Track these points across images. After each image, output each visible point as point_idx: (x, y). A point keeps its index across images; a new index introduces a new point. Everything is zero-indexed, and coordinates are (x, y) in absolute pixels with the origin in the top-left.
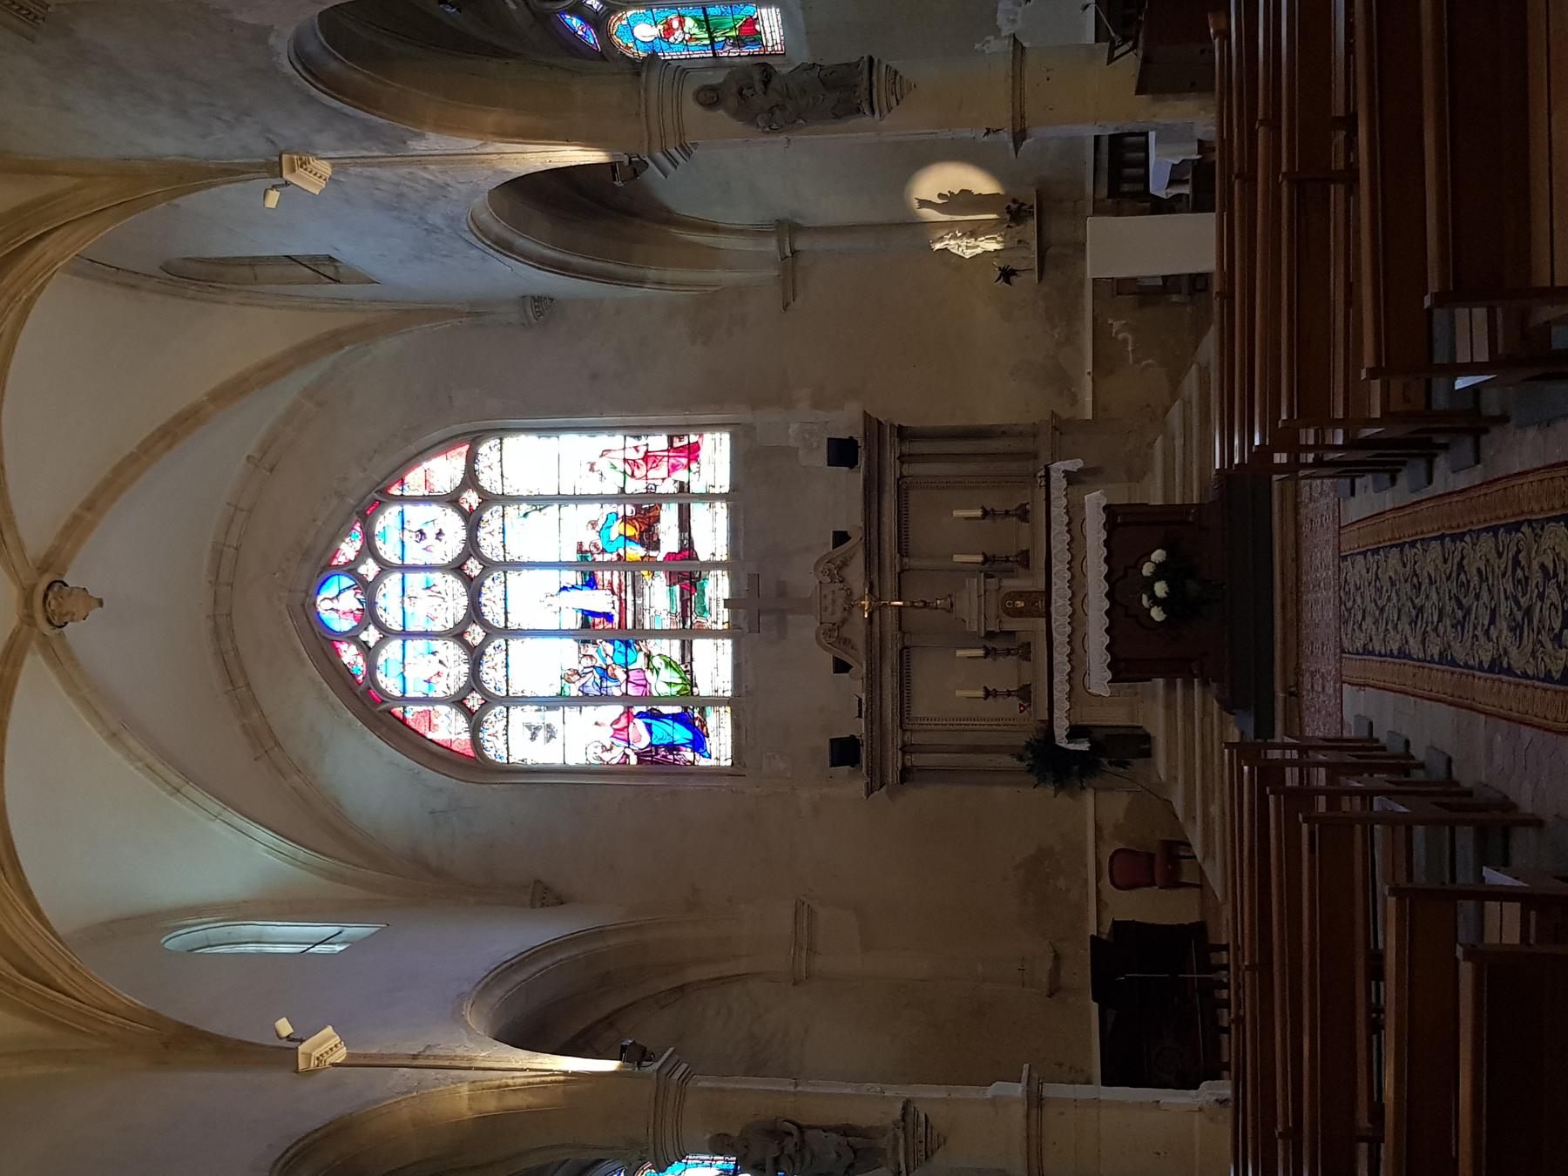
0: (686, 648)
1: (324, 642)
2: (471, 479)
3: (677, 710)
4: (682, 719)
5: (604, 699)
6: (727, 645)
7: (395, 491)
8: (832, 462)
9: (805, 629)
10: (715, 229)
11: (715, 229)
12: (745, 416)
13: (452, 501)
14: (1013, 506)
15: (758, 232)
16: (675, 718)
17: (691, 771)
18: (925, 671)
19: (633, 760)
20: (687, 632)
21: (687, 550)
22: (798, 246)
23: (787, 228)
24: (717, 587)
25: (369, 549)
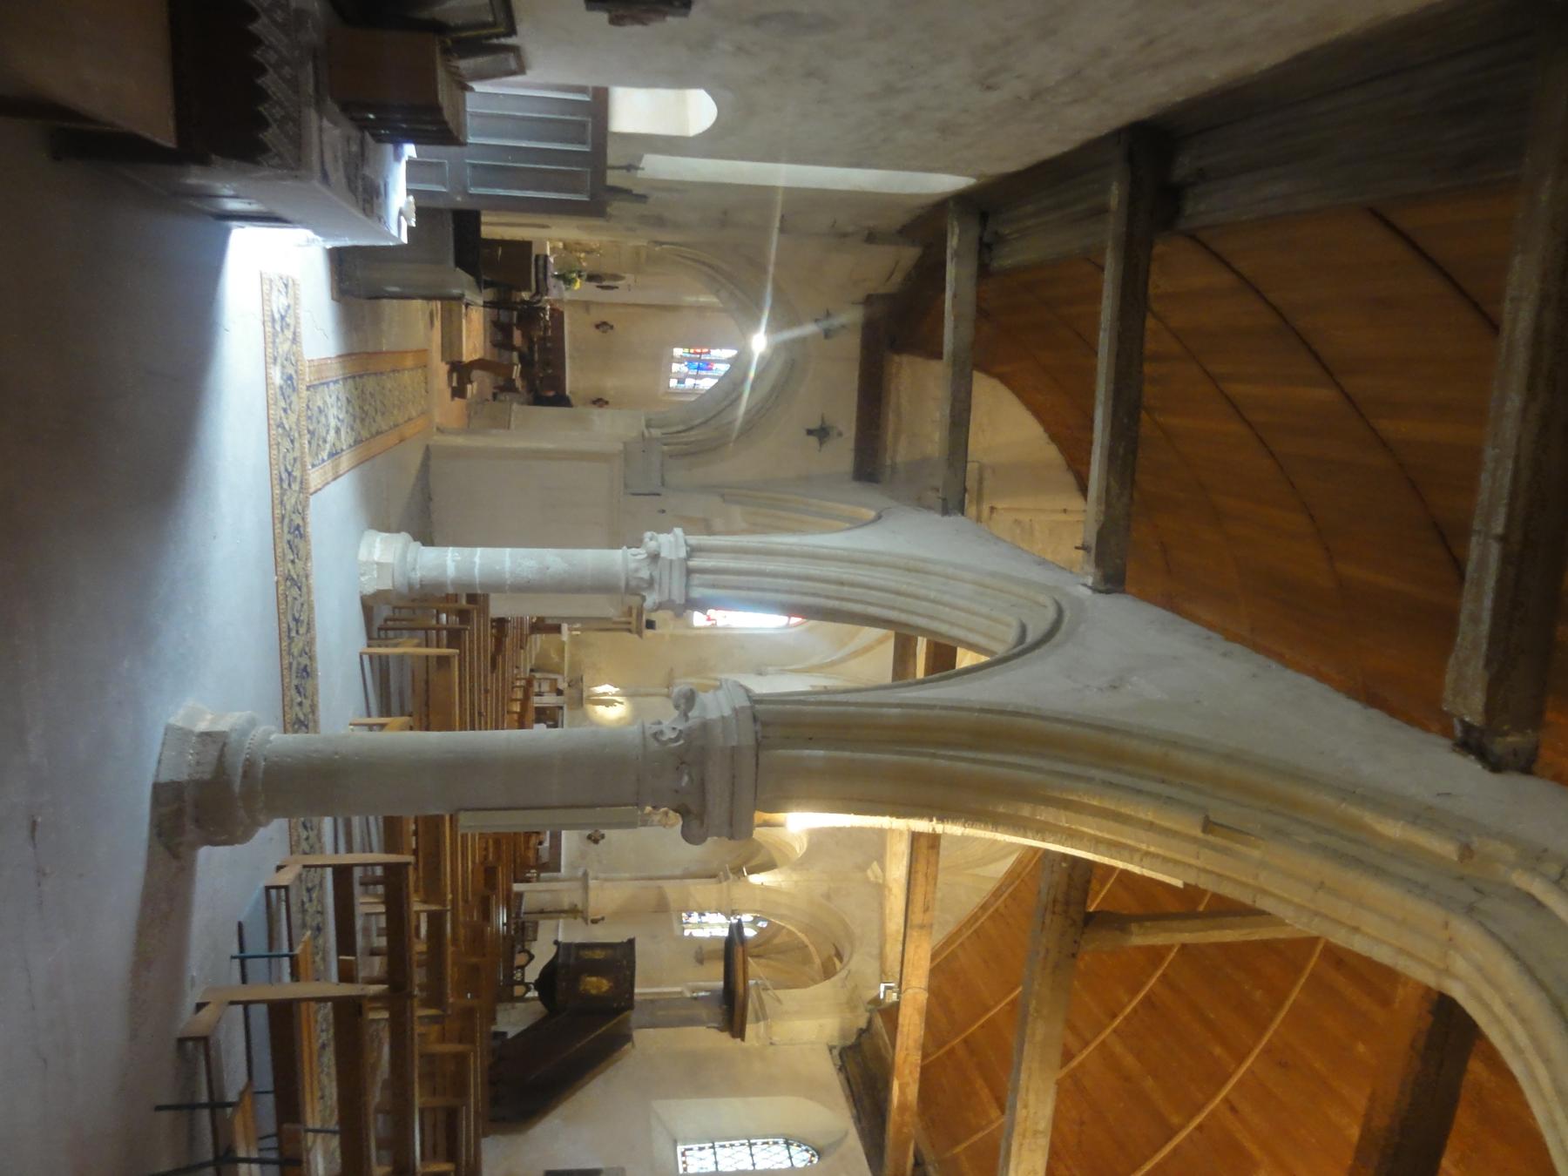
12: (689, 632)
22: (666, 690)
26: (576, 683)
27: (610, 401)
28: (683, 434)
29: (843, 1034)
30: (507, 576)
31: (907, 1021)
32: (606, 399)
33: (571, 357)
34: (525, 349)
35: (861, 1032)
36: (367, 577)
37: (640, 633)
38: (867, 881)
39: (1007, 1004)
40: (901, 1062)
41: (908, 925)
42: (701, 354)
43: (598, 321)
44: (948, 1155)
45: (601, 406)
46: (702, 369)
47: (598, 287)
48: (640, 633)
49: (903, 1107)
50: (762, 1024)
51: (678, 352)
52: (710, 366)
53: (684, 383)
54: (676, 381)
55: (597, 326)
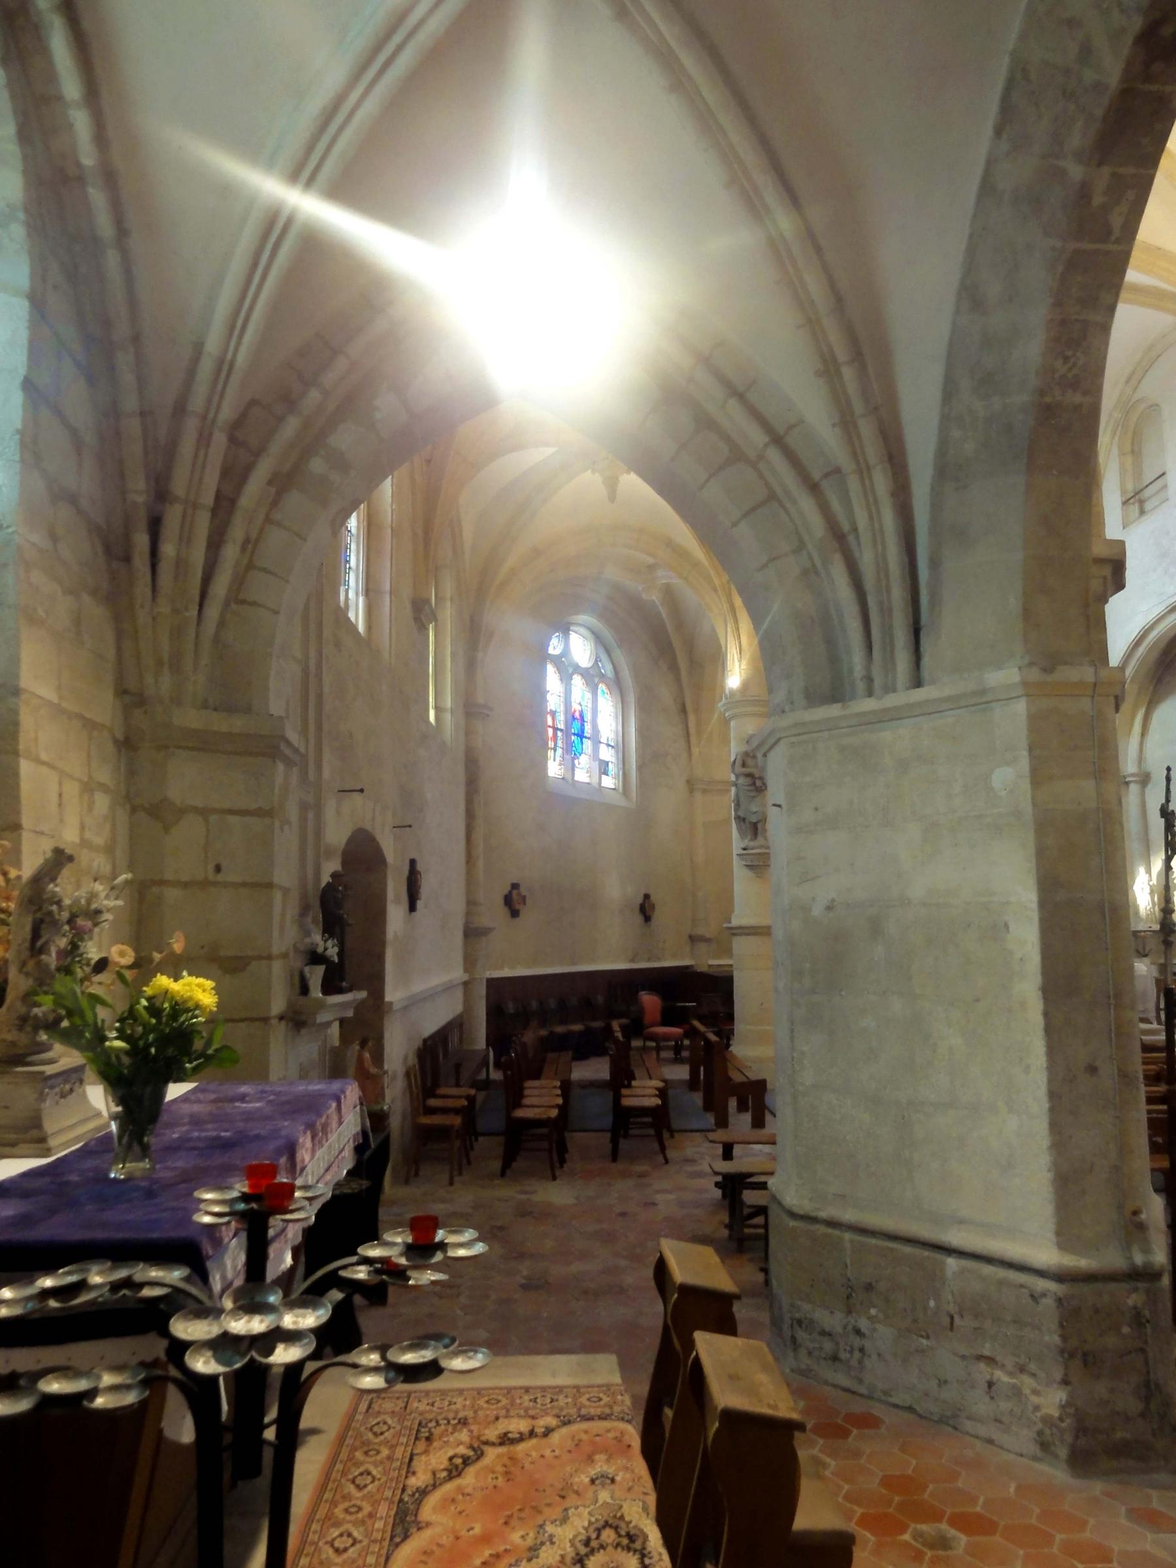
10: (1144, 733)
11: (1144, 733)
27: (643, 892)
28: (867, 560)
32: (640, 900)
33: (574, 964)
34: (567, 1055)
42: (555, 729)
43: (502, 911)
45: (653, 907)
46: (582, 730)
47: (412, 908)
51: (554, 769)
52: (577, 715)
53: (607, 763)
54: (604, 777)
55: (515, 914)
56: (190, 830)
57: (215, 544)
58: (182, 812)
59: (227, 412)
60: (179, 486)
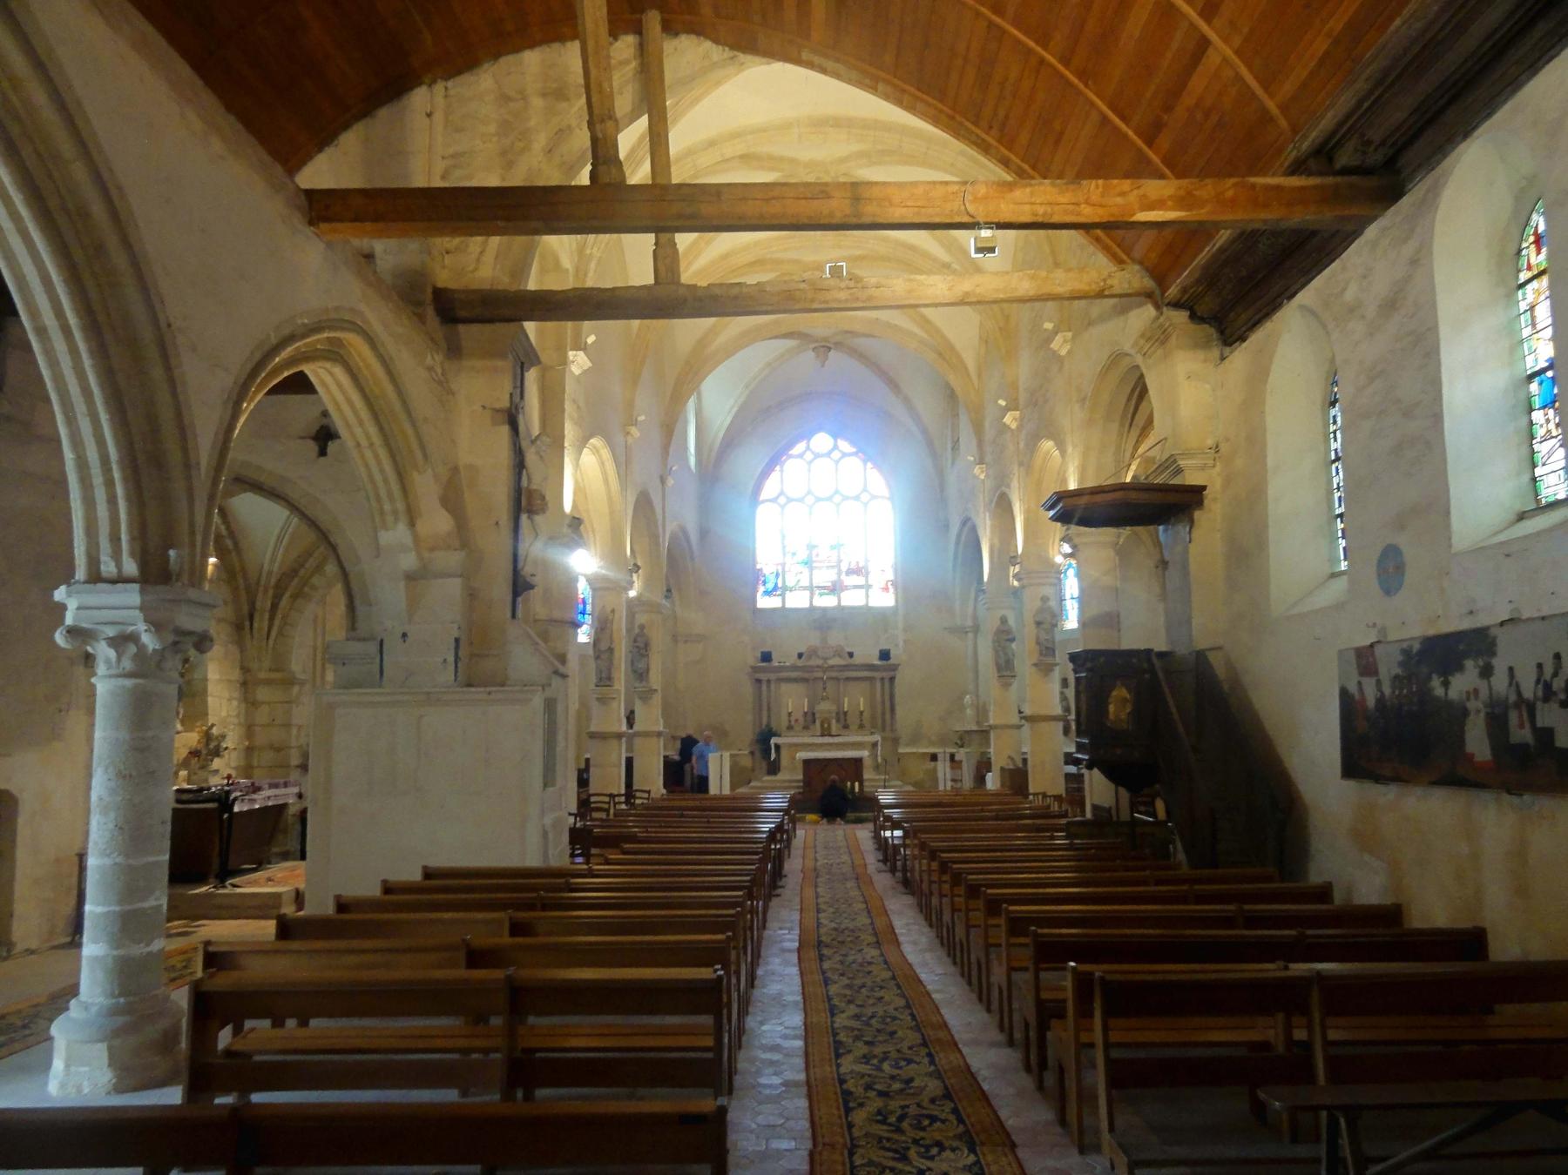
0: (805, 588)
1: (807, 436)
2: (874, 497)
3: (780, 585)
4: (776, 588)
5: (784, 554)
6: (807, 605)
7: (869, 465)
8: (881, 651)
9: (814, 640)
13: (865, 490)
14: (864, 722)
15: (975, 617)
16: (776, 584)
17: (755, 591)
18: (799, 688)
19: (758, 567)
20: (811, 589)
21: (846, 588)
23: (976, 629)
24: (828, 601)
25: (844, 455)
26: (963, 739)
29: (1205, 345)
30: (108, 861)
31: (1027, 208)
35: (1194, 317)
36: (86, 1083)
37: (895, 668)
38: (1069, 352)
39: (1086, 85)
40: (1100, 211)
41: (854, 221)
44: (1283, 123)
48: (895, 668)
49: (1183, 201)
50: (1182, 463)
56: (265, 709)
57: (272, 619)
58: (263, 703)
59: (273, 581)
60: (258, 604)
